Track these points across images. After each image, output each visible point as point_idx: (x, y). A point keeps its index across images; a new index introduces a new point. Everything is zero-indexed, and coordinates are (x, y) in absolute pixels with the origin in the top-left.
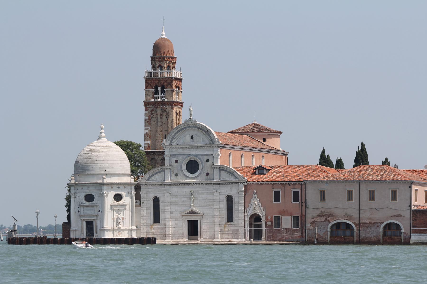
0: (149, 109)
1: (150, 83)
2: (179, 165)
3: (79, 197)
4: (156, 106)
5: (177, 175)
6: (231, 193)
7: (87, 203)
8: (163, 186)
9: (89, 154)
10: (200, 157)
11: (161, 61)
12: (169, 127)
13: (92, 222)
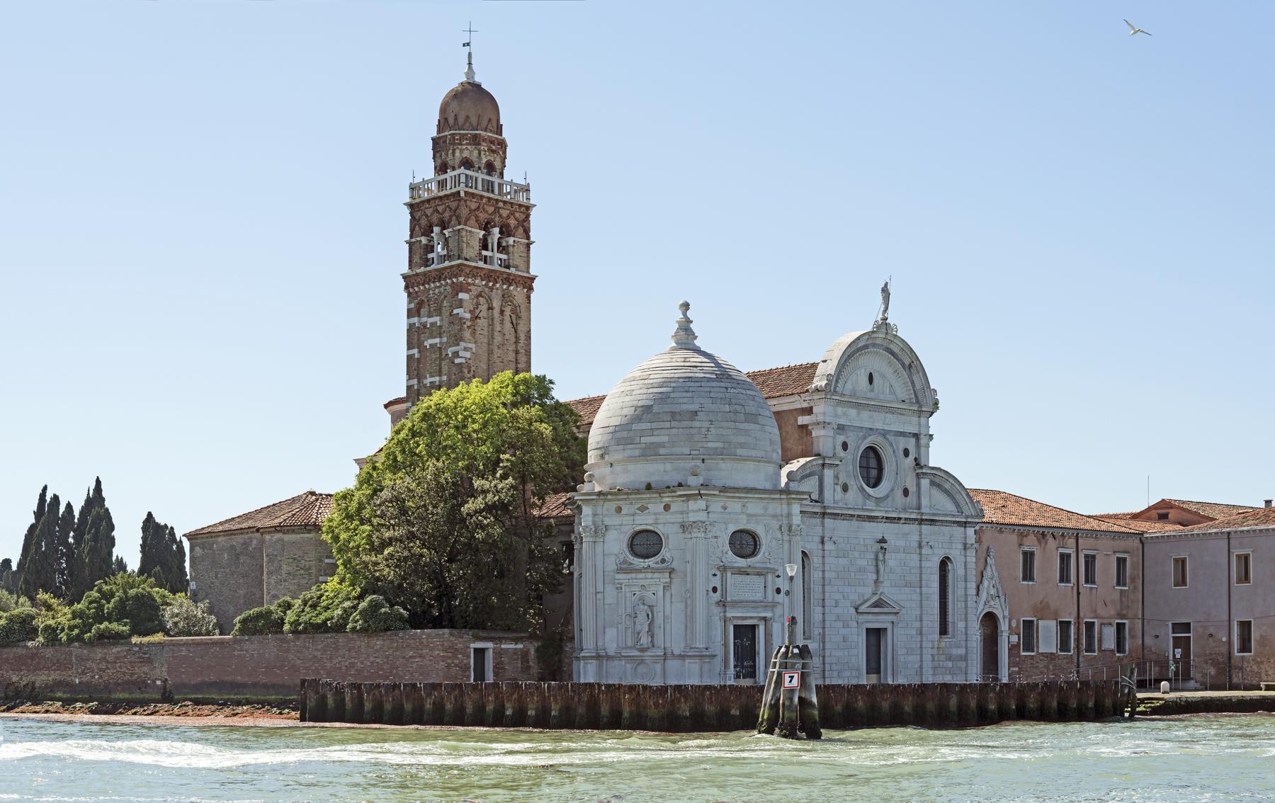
0: (471, 287)
1: (474, 210)
2: (849, 457)
3: (716, 537)
4: (491, 284)
5: (845, 488)
6: (952, 552)
7: (741, 562)
8: (818, 521)
9: (727, 388)
10: (891, 438)
12: (521, 351)
13: (753, 628)
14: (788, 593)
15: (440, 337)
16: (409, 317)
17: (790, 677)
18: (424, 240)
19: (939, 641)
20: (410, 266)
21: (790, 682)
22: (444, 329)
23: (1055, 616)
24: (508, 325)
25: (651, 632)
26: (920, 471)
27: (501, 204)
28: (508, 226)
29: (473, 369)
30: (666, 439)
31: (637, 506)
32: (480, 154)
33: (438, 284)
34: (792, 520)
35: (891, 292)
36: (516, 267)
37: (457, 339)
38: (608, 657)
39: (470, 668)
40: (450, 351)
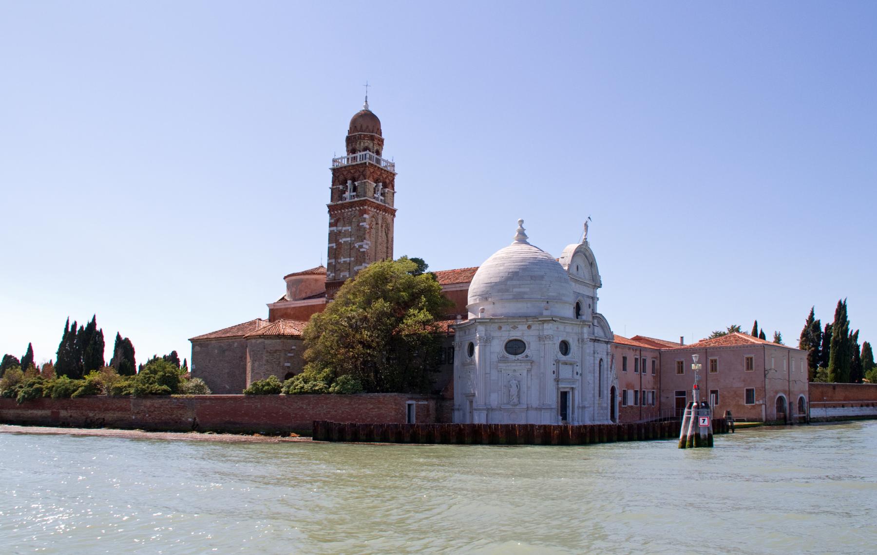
7: (564, 358)
11: (379, 145)
14: (581, 375)
15: (351, 238)
16: (330, 227)
17: (703, 419)
18: (341, 187)
19: (599, 400)
20: (332, 200)
21: (703, 422)
22: (353, 233)
23: (632, 387)
24: (384, 234)
25: (519, 396)
26: (594, 315)
27: (383, 171)
28: (386, 182)
29: (369, 254)
30: (528, 290)
31: (511, 326)
32: (374, 145)
33: (350, 210)
34: (584, 336)
35: (589, 225)
36: (388, 204)
37: (362, 239)
38: (492, 409)
39: (406, 415)
40: (357, 245)
